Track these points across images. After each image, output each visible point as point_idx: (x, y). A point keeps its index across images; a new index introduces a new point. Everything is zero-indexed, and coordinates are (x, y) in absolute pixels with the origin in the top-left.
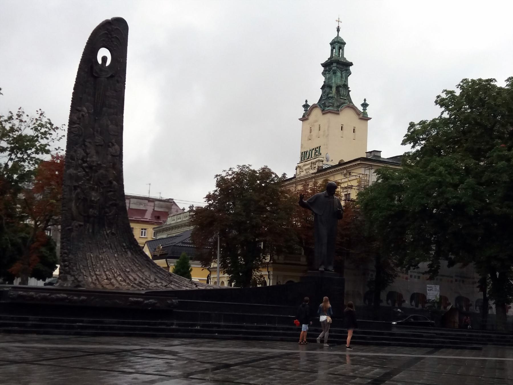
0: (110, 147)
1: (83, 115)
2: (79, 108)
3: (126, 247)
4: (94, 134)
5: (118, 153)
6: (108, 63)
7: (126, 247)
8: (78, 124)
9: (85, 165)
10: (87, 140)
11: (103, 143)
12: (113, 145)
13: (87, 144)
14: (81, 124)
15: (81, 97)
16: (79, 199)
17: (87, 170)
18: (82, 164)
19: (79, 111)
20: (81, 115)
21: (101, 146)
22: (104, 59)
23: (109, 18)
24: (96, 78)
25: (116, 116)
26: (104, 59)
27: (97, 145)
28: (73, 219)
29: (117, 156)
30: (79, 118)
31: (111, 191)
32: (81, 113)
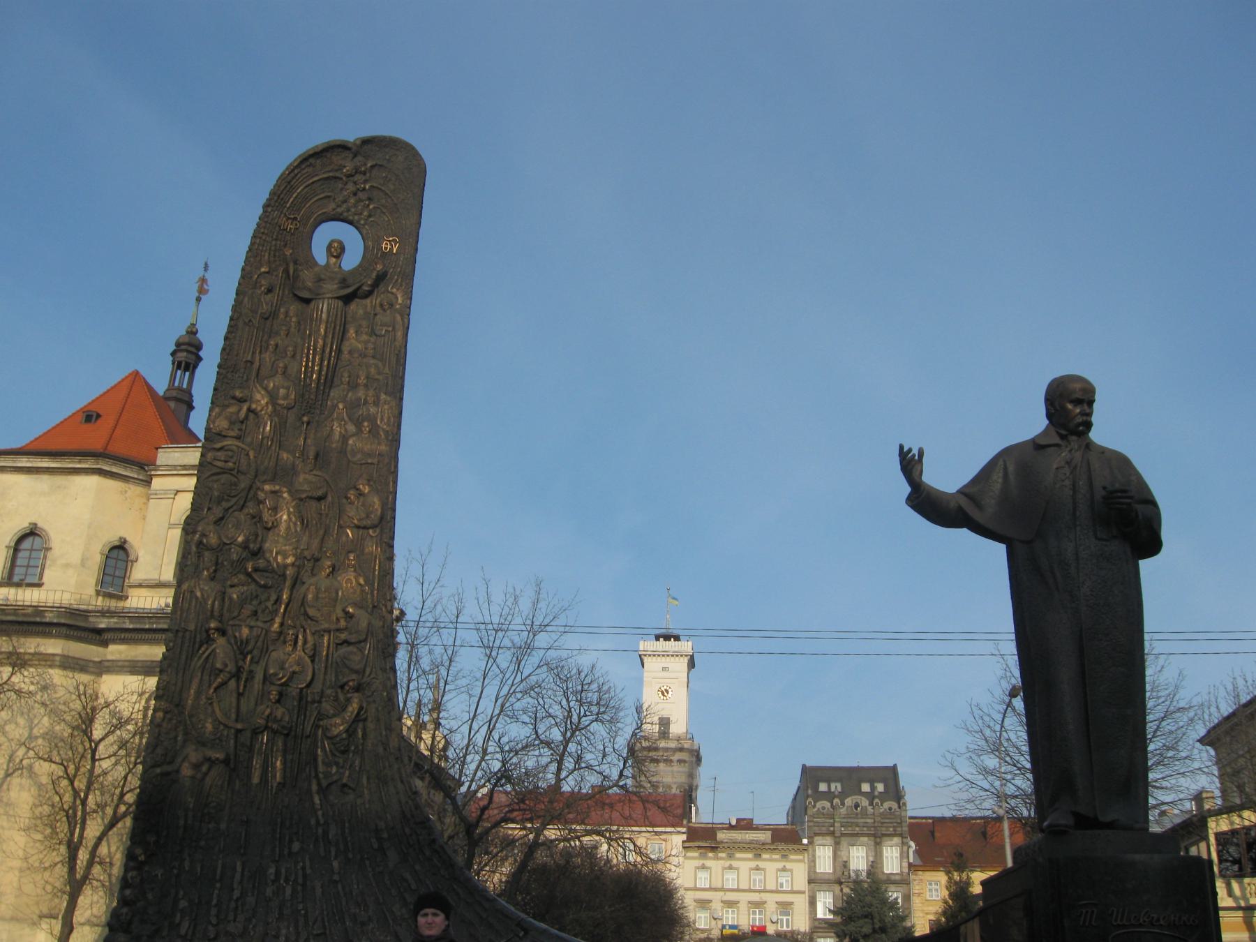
0: (352, 503)
2: (238, 394)
3: (385, 835)
4: (294, 467)
5: (375, 517)
6: (352, 260)
7: (385, 835)
8: (238, 438)
10: (267, 487)
12: (361, 494)
13: (261, 495)
14: (249, 440)
15: (249, 358)
16: (221, 671)
18: (241, 561)
19: (241, 401)
21: (319, 499)
22: (336, 250)
23: (351, 135)
24: (307, 301)
25: (372, 410)
26: (336, 250)
27: (301, 500)
29: (374, 527)
31: (346, 642)
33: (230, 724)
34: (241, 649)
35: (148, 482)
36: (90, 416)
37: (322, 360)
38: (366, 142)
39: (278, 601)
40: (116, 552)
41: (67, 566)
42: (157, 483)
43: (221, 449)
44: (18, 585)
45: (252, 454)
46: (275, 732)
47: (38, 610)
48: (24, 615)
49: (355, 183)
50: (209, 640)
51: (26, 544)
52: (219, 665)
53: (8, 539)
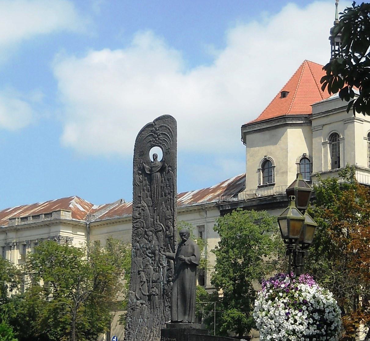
1: (142, 209)
6: (160, 158)
8: (139, 218)
9: (148, 251)
11: (161, 228)
15: (140, 195)
16: (141, 282)
17: (150, 255)
19: (140, 207)
20: (141, 211)
23: (151, 120)
26: (155, 156)
28: (138, 299)
29: (172, 237)
30: (140, 214)
32: (141, 208)
33: (145, 294)
34: (148, 274)
35: (311, 123)
36: (284, 94)
37: (156, 191)
38: (157, 120)
39: (155, 260)
40: (303, 161)
41: (283, 173)
42: (314, 123)
43: (137, 222)
44: (266, 186)
45: (144, 221)
46: (154, 295)
47: (272, 197)
48: (269, 200)
49: (156, 134)
50: (140, 274)
51: (266, 166)
52: (142, 280)
53: (258, 165)
